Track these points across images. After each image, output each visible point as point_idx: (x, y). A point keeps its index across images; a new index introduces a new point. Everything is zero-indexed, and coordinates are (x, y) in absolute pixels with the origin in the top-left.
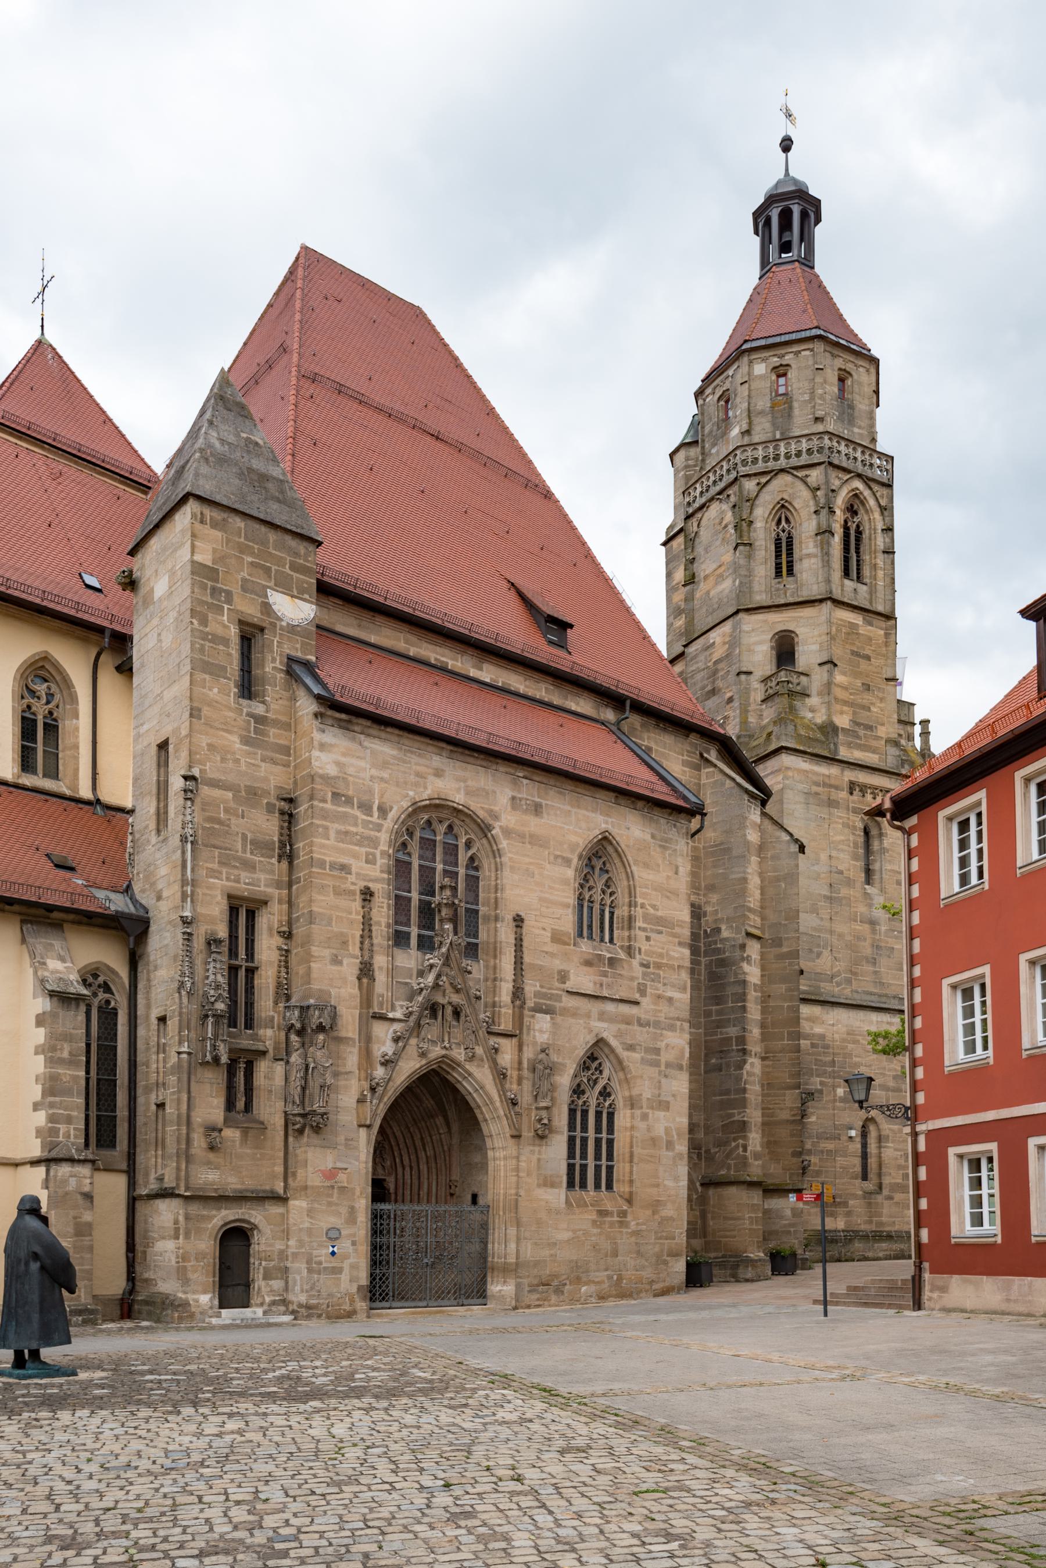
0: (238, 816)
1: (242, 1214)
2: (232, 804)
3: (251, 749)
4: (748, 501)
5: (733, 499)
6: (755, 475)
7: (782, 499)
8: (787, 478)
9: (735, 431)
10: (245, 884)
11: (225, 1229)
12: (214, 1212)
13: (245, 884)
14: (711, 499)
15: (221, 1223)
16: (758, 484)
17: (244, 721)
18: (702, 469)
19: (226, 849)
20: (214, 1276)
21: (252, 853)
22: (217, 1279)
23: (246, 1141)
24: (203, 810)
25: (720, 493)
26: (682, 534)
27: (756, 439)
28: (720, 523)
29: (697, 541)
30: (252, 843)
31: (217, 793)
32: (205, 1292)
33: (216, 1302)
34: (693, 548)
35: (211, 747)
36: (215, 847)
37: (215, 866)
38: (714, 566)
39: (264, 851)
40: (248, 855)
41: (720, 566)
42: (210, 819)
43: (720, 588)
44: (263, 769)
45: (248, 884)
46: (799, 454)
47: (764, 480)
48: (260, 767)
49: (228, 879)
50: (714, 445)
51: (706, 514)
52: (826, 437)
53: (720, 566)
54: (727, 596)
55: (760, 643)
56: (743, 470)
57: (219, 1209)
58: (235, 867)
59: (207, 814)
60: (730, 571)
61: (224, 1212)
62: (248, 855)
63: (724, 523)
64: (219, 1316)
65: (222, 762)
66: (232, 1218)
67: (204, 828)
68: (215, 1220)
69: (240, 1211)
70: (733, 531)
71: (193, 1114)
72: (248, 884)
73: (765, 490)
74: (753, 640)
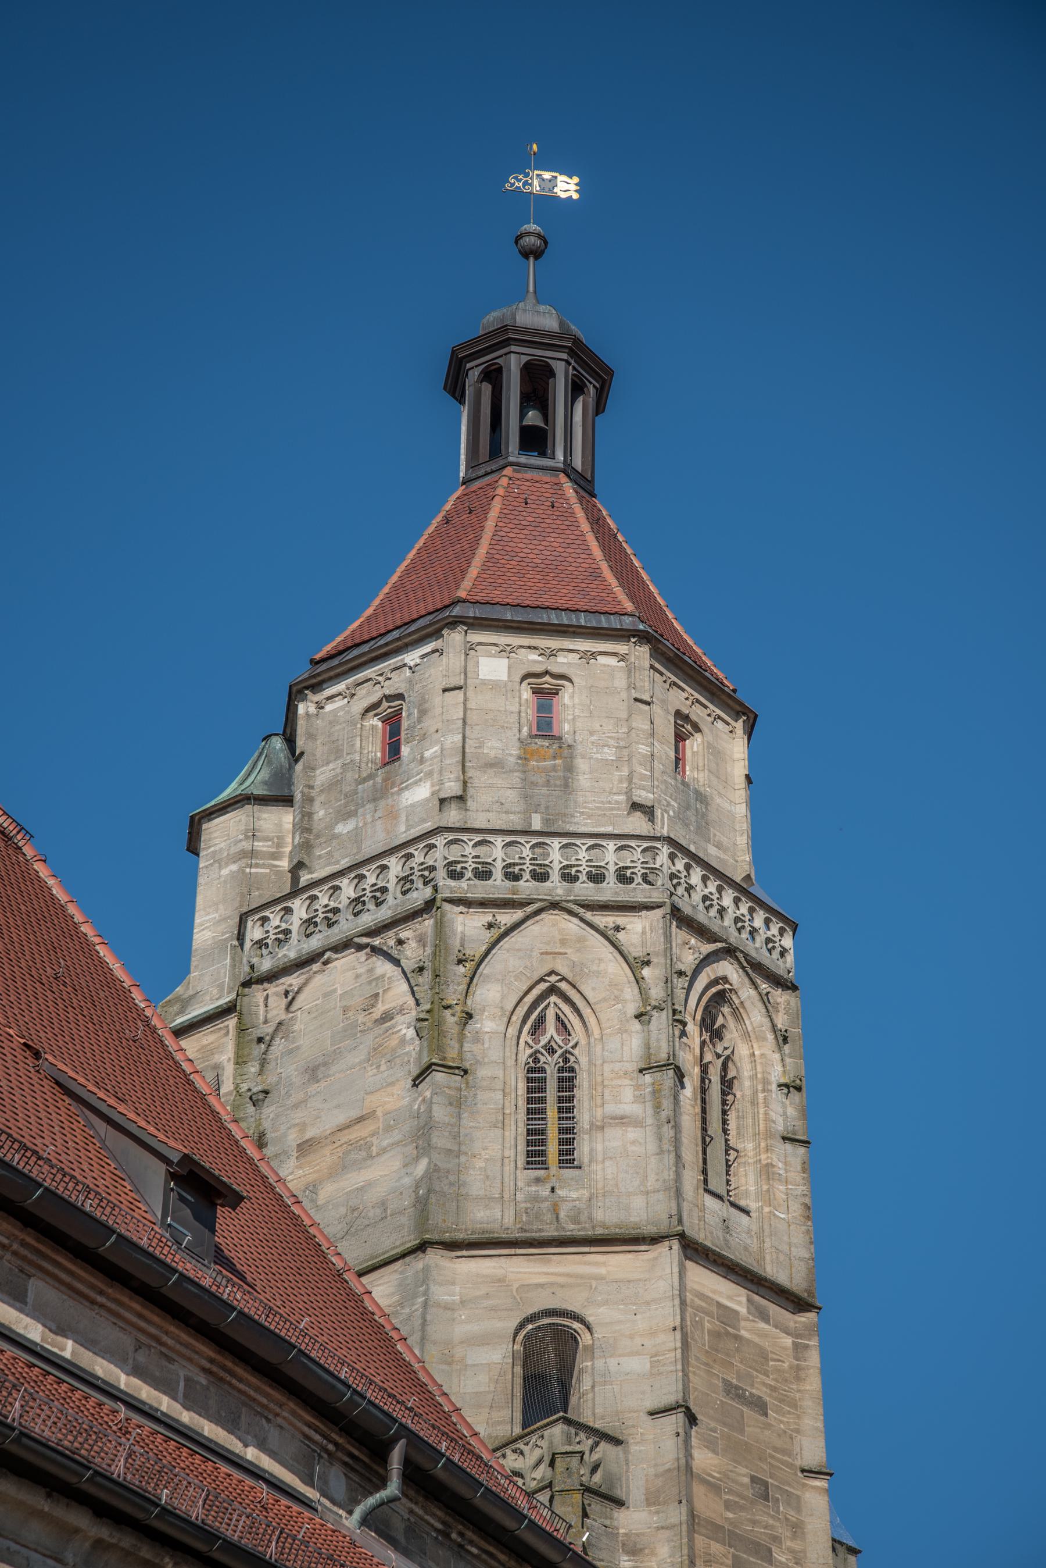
4: (460, 962)
5: (412, 954)
6: (483, 904)
7: (552, 973)
8: (571, 926)
9: (420, 793)
14: (344, 946)
16: (490, 926)
18: (298, 867)
25: (371, 933)
26: (231, 1022)
27: (480, 821)
28: (367, 1009)
29: (279, 1046)
34: (263, 1063)
38: (341, 1118)
41: (361, 1119)
43: (355, 1179)
46: (596, 877)
47: (506, 918)
50: (346, 815)
51: (318, 980)
52: (665, 850)
53: (361, 1119)
54: (383, 1204)
55: (484, 1340)
56: (448, 886)
60: (396, 1136)
63: (380, 1009)
70: (411, 1033)
73: (505, 943)
74: (460, 1330)
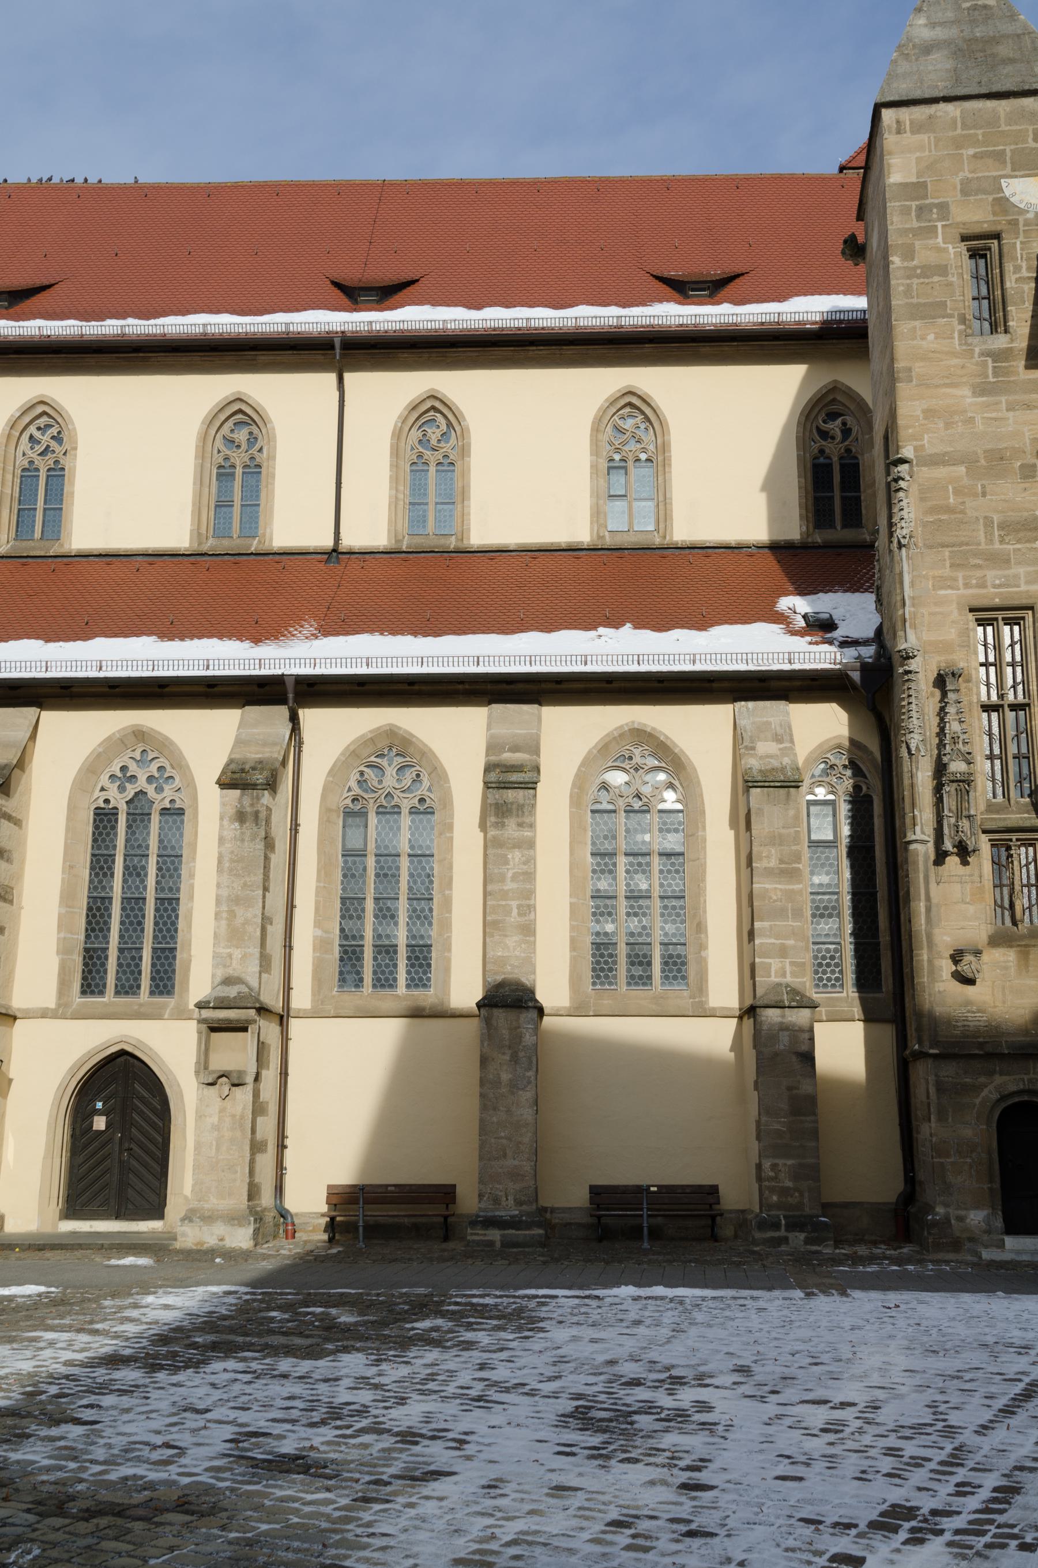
0: (976, 495)
1: (1030, 1081)
2: (966, 481)
3: (991, 399)
10: (995, 586)
11: (1003, 1105)
12: (982, 1079)
13: (995, 586)
15: (995, 1096)
17: (977, 364)
19: (961, 544)
20: (991, 1181)
21: (1002, 542)
22: (997, 1185)
23: (1027, 966)
24: (922, 499)
30: (1002, 526)
31: (941, 472)
32: (977, 1208)
33: (999, 1223)
35: (930, 413)
36: (943, 546)
37: (947, 572)
39: (1021, 535)
40: (997, 546)
42: (933, 510)
44: (1011, 421)
45: (1000, 586)
48: (1008, 419)
49: (967, 586)
57: (991, 1073)
58: (978, 567)
59: (929, 504)
61: (998, 1080)
62: (997, 546)
64: (1001, 1245)
65: (946, 429)
66: (1013, 1088)
67: (925, 525)
68: (985, 1092)
69: (1026, 1077)
71: (936, 931)
72: (1000, 586)
